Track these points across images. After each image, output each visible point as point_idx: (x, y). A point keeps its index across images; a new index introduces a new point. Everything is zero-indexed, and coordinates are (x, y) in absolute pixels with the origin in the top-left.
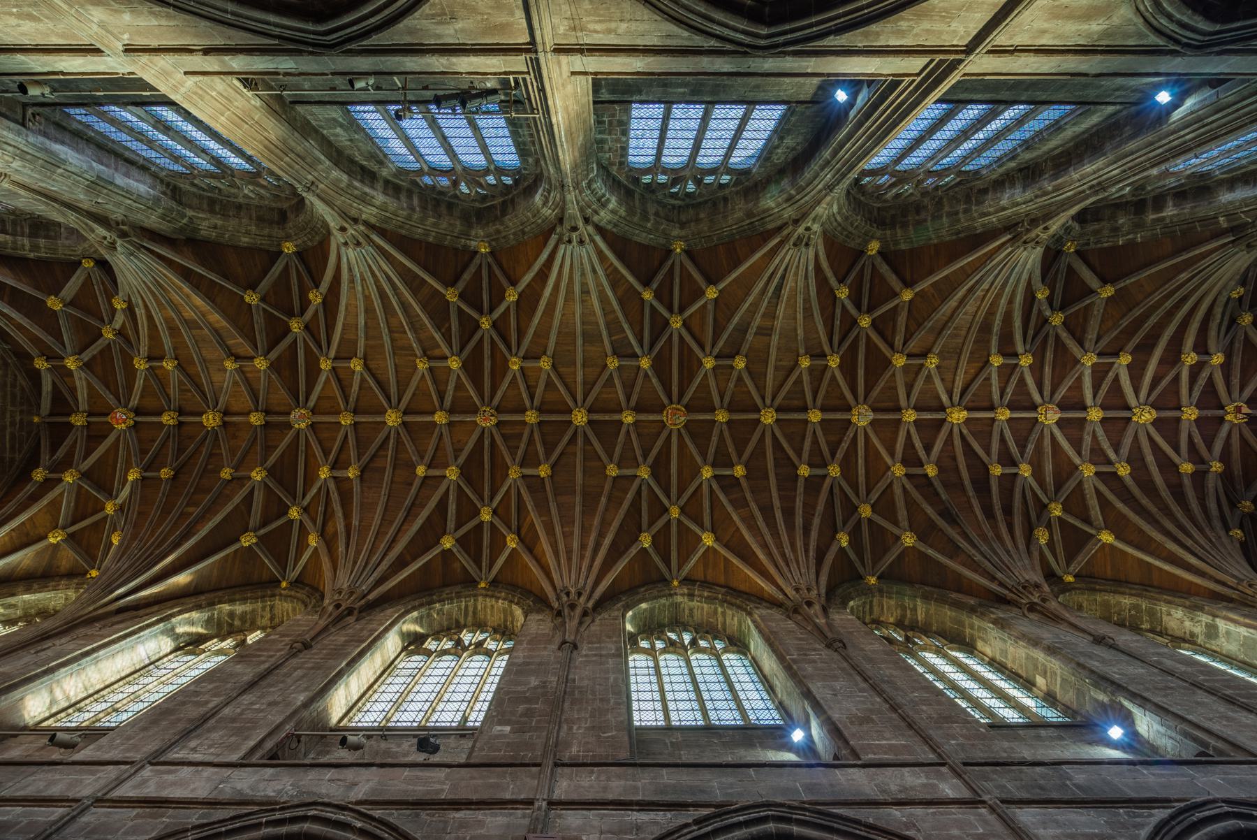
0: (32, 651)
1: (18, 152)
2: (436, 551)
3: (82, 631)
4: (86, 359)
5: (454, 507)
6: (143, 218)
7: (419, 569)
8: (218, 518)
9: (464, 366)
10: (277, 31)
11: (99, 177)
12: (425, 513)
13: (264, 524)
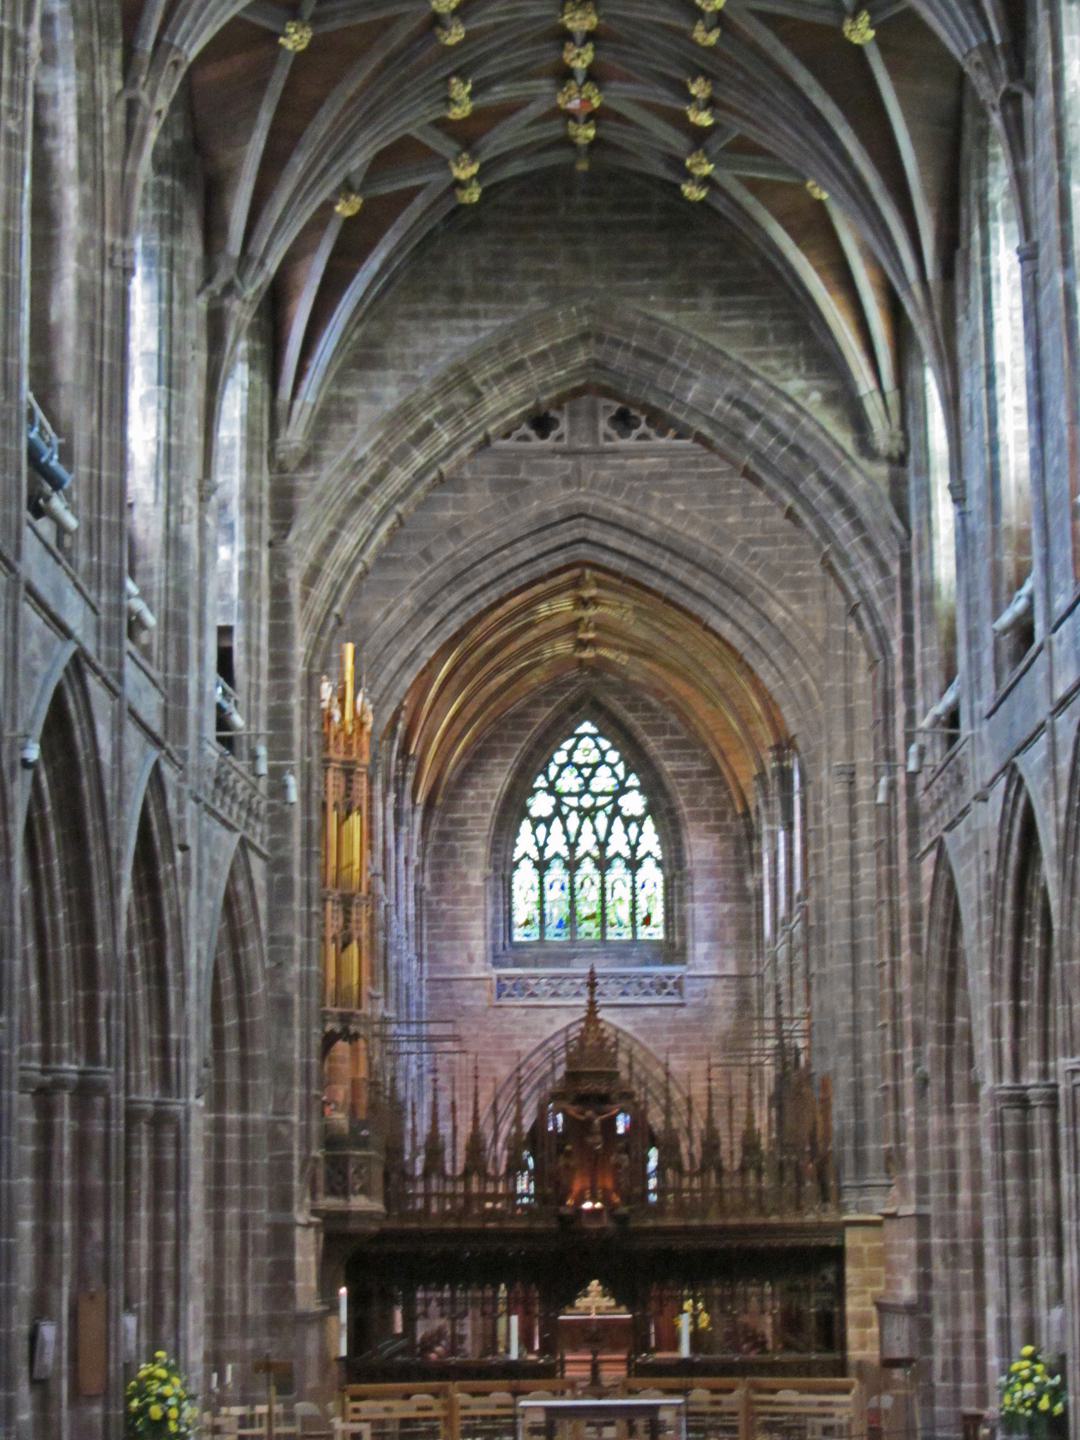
0: (968, 429)
1: (172, 507)
3: (962, 347)
4: (456, 147)
6: (191, 266)
8: (803, 78)
10: (77, 688)
11: (159, 383)
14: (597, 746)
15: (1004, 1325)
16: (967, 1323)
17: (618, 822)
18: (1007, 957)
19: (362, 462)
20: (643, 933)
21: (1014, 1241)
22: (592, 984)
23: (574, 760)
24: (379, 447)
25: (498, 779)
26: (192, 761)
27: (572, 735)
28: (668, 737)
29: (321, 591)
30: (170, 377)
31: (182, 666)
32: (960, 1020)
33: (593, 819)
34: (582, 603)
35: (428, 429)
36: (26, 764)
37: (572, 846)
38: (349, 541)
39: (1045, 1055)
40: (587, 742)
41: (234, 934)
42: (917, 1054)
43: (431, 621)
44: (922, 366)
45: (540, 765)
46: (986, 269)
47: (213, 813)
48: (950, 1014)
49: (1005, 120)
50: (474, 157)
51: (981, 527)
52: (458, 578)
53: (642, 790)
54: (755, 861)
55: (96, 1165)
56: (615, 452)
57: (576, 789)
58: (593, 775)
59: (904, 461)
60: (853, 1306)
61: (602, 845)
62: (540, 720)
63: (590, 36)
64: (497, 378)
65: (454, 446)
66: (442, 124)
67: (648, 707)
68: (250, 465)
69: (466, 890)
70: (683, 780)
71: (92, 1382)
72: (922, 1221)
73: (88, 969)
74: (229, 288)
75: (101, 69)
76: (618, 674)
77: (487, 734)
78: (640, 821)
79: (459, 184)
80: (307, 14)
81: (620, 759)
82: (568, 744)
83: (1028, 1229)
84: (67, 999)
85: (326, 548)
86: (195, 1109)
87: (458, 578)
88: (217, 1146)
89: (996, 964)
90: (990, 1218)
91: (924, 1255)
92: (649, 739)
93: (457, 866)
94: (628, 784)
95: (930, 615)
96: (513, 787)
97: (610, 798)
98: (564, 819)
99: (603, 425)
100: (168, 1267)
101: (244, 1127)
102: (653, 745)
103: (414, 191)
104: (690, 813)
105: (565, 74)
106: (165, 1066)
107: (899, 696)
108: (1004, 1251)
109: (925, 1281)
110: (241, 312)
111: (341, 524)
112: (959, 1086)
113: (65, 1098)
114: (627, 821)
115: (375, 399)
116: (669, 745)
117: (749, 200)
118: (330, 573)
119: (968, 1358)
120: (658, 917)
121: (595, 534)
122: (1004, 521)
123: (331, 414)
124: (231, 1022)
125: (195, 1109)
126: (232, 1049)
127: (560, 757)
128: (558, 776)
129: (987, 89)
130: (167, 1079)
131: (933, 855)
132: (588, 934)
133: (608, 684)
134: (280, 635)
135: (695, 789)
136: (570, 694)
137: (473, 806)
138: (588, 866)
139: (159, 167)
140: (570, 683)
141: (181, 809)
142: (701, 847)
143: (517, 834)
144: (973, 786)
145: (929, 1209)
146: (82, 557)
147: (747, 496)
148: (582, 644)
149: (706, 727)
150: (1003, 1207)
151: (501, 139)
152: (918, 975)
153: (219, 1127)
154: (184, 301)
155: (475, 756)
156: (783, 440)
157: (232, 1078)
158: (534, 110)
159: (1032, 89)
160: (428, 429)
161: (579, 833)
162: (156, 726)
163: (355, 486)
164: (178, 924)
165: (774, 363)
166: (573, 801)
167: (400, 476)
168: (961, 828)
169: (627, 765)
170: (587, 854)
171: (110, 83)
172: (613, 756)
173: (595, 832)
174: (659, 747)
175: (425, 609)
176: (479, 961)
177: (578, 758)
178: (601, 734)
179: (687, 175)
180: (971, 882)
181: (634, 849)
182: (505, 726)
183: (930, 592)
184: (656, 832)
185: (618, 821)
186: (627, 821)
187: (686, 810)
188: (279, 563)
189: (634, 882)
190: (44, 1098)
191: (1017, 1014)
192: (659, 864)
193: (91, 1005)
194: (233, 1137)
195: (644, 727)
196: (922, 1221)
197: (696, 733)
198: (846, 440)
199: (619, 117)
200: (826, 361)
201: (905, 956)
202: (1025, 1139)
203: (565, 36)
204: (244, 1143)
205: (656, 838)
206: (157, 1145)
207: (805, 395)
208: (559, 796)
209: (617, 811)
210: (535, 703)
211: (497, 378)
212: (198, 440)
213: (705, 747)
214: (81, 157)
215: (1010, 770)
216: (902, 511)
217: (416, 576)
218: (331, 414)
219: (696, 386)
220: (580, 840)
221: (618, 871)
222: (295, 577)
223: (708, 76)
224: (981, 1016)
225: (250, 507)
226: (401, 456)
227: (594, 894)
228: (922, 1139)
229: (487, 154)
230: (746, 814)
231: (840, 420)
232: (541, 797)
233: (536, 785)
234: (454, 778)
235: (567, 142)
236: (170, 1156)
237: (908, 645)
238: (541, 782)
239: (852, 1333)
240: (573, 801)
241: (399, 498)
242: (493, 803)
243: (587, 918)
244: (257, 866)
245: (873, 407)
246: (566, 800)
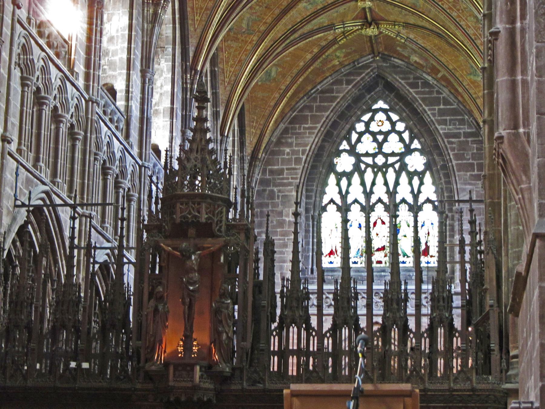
14: (389, 119)
17: (404, 178)
23: (371, 129)
27: (369, 110)
28: (442, 107)
33: (384, 175)
37: (368, 195)
40: (380, 116)
45: (344, 132)
53: (422, 152)
57: (371, 151)
58: (385, 140)
61: (392, 194)
62: (341, 95)
67: (426, 84)
70: (453, 140)
76: (401, 57)
77: (301, 105)
78: (421, 175)
81: (406, 128)
82: (366, 117)
92: (426, 108)
93: (275, 205)
94: (413, 147)
96: (321, 148)
97: (398, 158)
98: (362, 174)
104: (457, 164)
114: (411, 175)
116: (442, 113)
127: (360, 127)
128: (359, 140)
132: (379, 262)
133: (395, 67)
135: (463, 146)
136: (366, 76)
137: (290, 160)
140: (366, 66)
143: (326, 184)
149: (470, 95)
155: (290, 123)
161: (373, 184)
166: (369, 160)
169: (411, 132)
170: (380, 200)
172: (400, 126)
173: (386, 184)
174: (434, 115)
177: (374, 127)
178: (392, 109)
181: (416, 197)
182: (315, 99)
184: (434, 183)
185: (404, 174)
186: (411, 175)
187: (454, 162)
189: (416, 222)
192: (435, 208)
195: (423, 100)
197: (462, 103)
205: (433, 188)
208: (358, 157)
209: (404, 167)
210: (338, 82)
213: (470, 113)
220: (375, 189)
232: (344, 155)
233: (341, 148)
234: (274, 139)
238: (345, 145)
240: (369, 160)
242: (304, 157)
243: (378, 250)
246: (363, 159)
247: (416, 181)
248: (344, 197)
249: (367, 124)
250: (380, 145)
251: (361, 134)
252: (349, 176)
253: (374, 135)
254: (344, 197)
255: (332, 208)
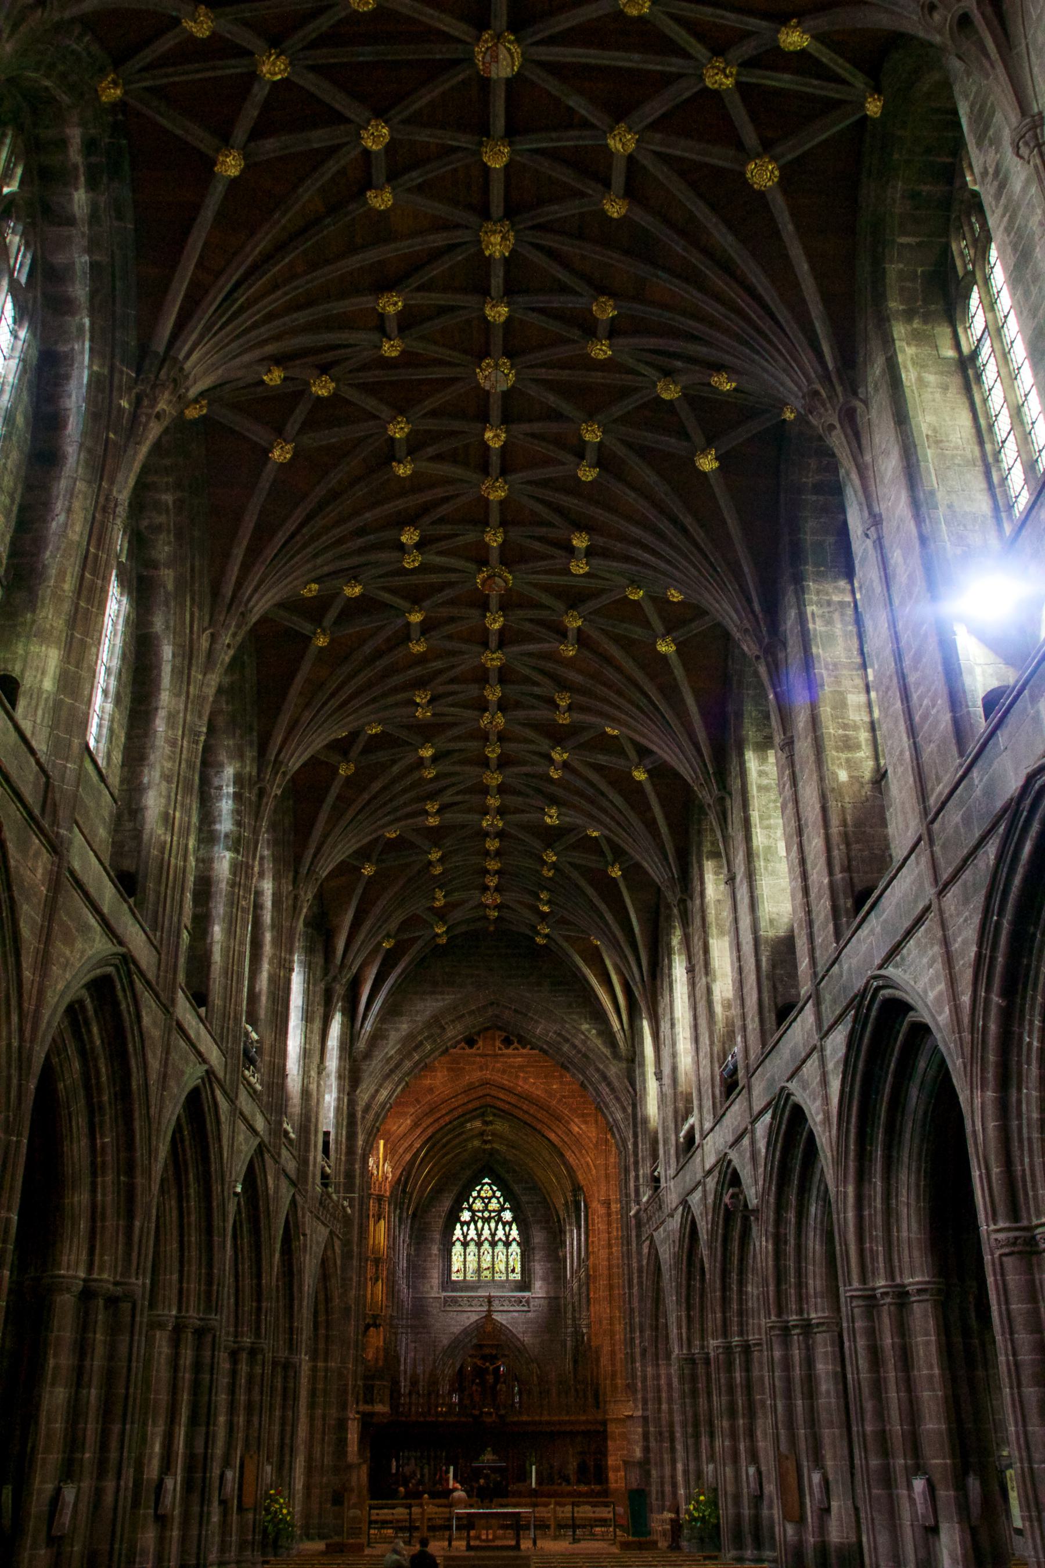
2: (648, 788)
3: (660, 1011)
5: (600, 757)
7: (663, 806)
8: (590, 891)
9: (427, 740)
12: (604, 787)
13: (602, 854)
15: (686, 1472)
16: (667, 1471)
17: (500, 1226)
18: (684, 1291)
19: (391, 1057)
20: (512, 1277)
21: (690, 1430)
22: (490, 1302)
24: (399, 1051)
25: (447, 1204)
26: (309, 1194)
29: (371, 1116)
30: (307, 1017)
31: (307, 1150)
32: (662, 1320)
34: (486, 1123)
35: (421, 1043)
36: (236, 1194)
37: (479, 1235)
38: (384, 1094)
39: (702, 1339)
41: (324, 1277)
42: (641, 1337)
43: (419, 1131)
44: (641, 1019)
46: (670, 975)
47: (318, 1218)
48: (657, 1320)
49: (680, 911)
50: (445, 923)
51: (668, 1090)
52: (432, 1111)
54: (563, 1243)
55: (257, 1389)
56: (502, 1055)
59: (633, 1060)
60: (611, 1461)
61: (493, 1235)
63: (497, 872)
64: (453, 1021)
65: (432, 1051)
66: (431, 909)
67: (515, 1171)
68: (340, 1058)
69: (430, 1255)
71: (249, 1500)
72: (645, 1419)
73: (258, 1294)
74: (335, 979)
75: (284, 881)
78: (510, 1224)
79: (438, 935)
80: (374, 859)
83: (696, 1425)
84: (248, 1306)
85: (373, 1097)
86: (304, 1360)
87: (432, 1111)
88: (313, 1379)
89: (678, 1294)
90: (677, 1418)
91: (646, 1436)
95: (646, 1130)
96: (452, 1207)
98: (476, 1223)
99: (498, 1043)
100: (287, 1441)
101: (326, 1370)
102: (516, 1188)
103: (419, 937)
105: (485, 888)
106: (291, 1340)
107: (632, 1167)
108: (685, 1434)
109: (646, 1449)
110: (340, 989)
111: (381, 1086)
112: (661, 1355)
113: (244, 1356)
115: (397, 1030)
117: (565, 945)
118: (375, 1108)
119: (668, 1488)
120: (518, 1269)
121: (493, 1093)
122: (680, 1089)
123: (377, 1037)
124: (322, 1318)
125: (304, 1360)
126: (322, 1331)
127: (475, 1194)
129: (671, 897)
130: (292, 1346)
131: (648, 1242)
134: (351, 1136)
138: (486, 1245)
139: (307, 924)
141: (304, 1216)
142: (538, 1237)
144: (667, 1211)
145: (649, 1413)
146: (265, 1098)
147: (561, 1076)
148: (486, 1142)
150: (684, 1413)
151: (457, 915)
152: (641, 1300)
153: (314, 1369)
154: (314, 985)
156: (579, 1051)
157: (322, 1346)
158: (472, 904)
159: (691, 898)
160: (421, 1043)
162: (294, 1177)
163: (387, 1069)
164: (301, 1272)
165: (575, 1017)
167: (408, 1064)
168: (661, 1229)
171: (287, 887)
172: (498, 1194)
175: (416, 1125)
176: (435, 1289)
177: (483, 1194)
178: (493, 1183)
179: (538, 933)
180: (666, 1253)
183: (645, 1121)
186: (504, 1224)
188: (352, 1103)
190: (234, 1356)
191: (689, 1318)
192: (519, 1244)
193: (259, 1309)
194: (321, 1374)
196: (645, 1419)
198: (607, 1051)
199: (508, 907)
200: (599, 1016)
201: (635, 1289)
202: (694, 1379)
203: (487, 872)
204: (326, 1377)
206: (285, 1378)
207: (589, 1031)
208: (473, 1212)
209: (500, 1219)
211: (453, 1021)
212: (318, 1046)
214: (272, 919)
215: (684, 1203)
216: (633, 1084)
217: (413, 1110)
218: (377, 1037)
219: (541, 1027)
221: (500, 1247)
222: (359, 1109)
223: (548, 890)
224: (672, 1319)
225: (340, 1077)
226: (409, 1055)
227: (489, 1258)
228: (644, 1379)
229: (450, 923)
230: (559, 1221)
231: (604, 1043)
235: (486, 918)
236: (291, 1385)
237: (635, 1145)
238: (465, 1205)
239: (611, 1475)
241: (407, 1074)
244: (337, 1243)
245: (620, 1036)
247: (507, 1228)
248: (465, 1237)
249: (479, 1192)
250: (487, 1205)
251: (475, 1198)
252: (468, 1224)
253: (483, 1198)
254: (465, 1237)
255: (458, 1244)
